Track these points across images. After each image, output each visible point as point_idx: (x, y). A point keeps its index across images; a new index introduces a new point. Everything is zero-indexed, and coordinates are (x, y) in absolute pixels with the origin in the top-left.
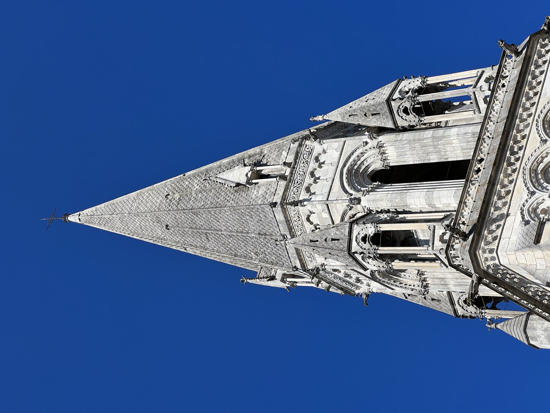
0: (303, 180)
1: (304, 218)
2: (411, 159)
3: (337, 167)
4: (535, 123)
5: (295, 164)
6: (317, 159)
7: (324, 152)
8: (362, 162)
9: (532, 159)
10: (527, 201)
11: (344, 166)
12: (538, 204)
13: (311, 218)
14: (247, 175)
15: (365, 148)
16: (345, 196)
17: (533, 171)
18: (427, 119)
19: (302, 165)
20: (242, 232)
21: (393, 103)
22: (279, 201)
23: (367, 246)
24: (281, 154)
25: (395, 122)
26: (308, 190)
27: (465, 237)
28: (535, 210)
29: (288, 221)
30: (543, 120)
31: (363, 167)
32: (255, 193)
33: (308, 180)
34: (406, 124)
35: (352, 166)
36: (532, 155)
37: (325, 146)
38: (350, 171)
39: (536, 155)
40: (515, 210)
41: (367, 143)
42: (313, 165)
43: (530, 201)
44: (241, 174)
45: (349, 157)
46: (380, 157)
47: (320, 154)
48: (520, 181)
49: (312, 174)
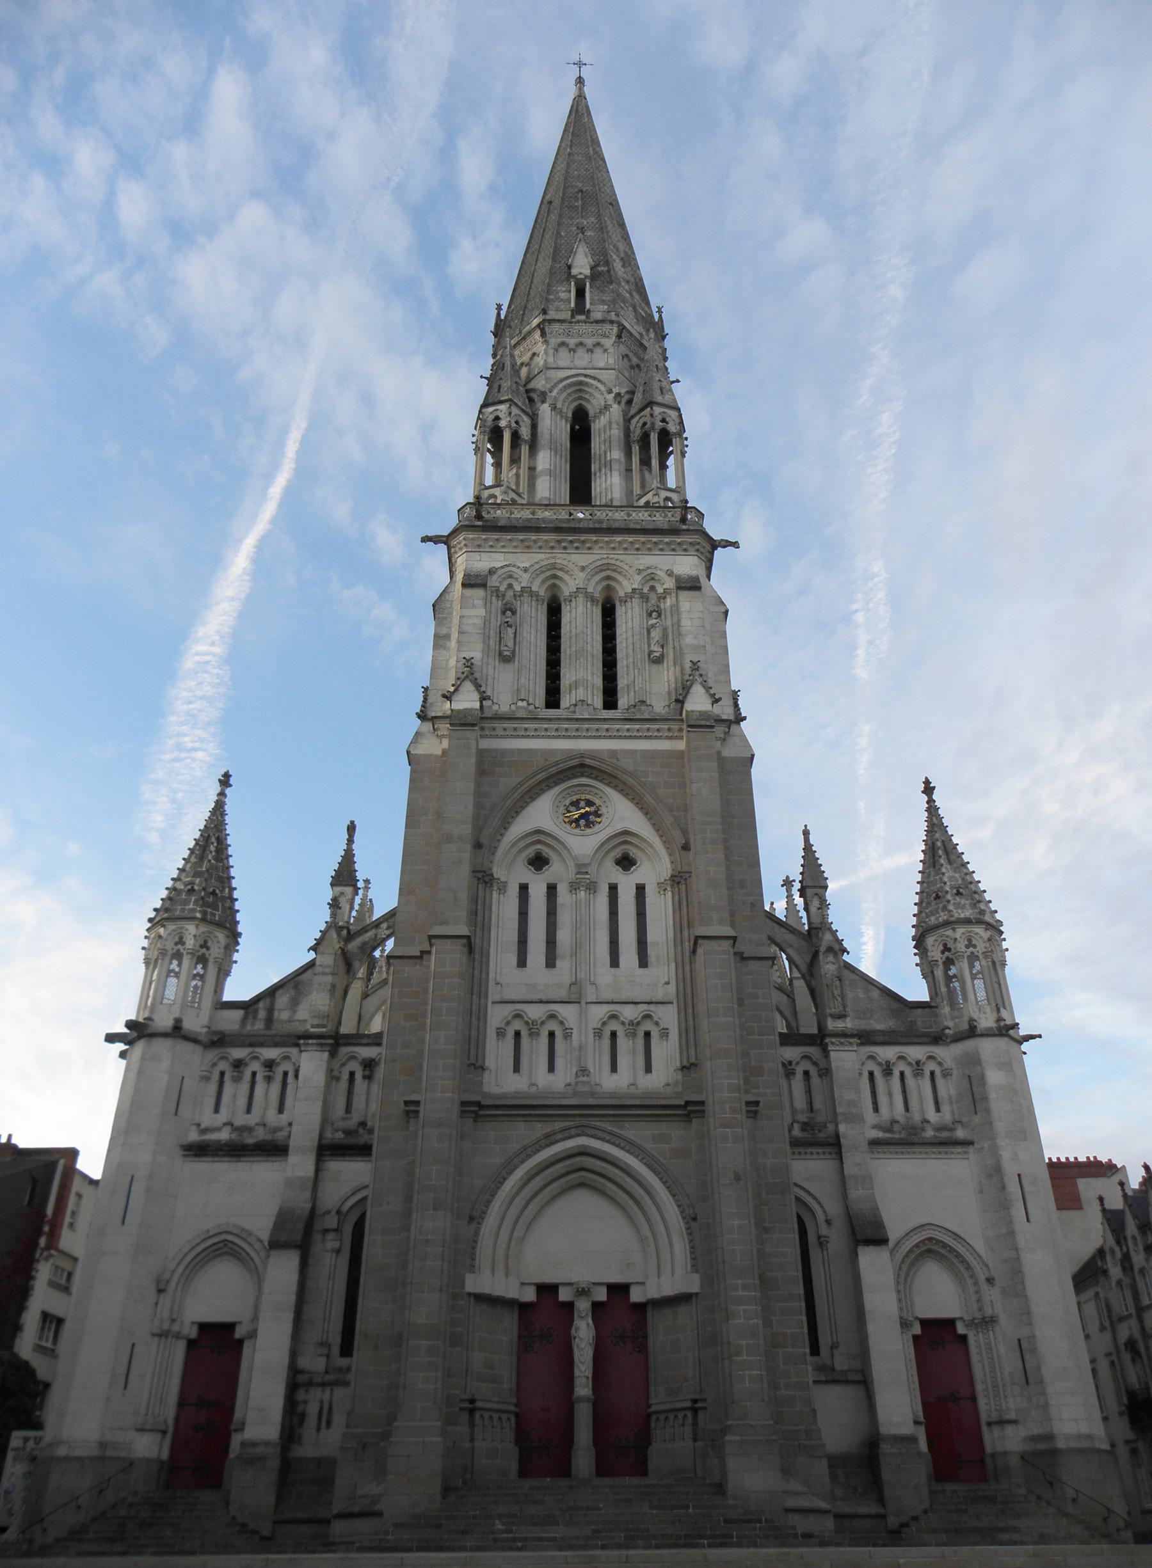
0: (573, 337)
1: (534, 350)
2: (597, 445)
3: (585, 369)
4: (605, 556)
5: (590, 323)
6: (598, 344)
7: (605, 350)
8: (591, 395)
9: (565, 563)
10: (519, 567)
11: (586, 376)
12: (517, 579)
13: (536, 358)
14: (581, 273)
15: (605, 393)
16: (548, 386)
17: (553, 567)
18: (636, 449)
19: (590, 330)
20: (530, 288)
21: (649, 409)
22: (548, 317)
23: (489, 423)
24: (607, 304)
25: (633, 417)
26: (563, 344)
27: (479, 517)
28: (511, 577)
29: (530, 333)
30: (608, 564)
31: (587, 396)
32: (564, 289)
33: (572, 342)
34: (632, 428)
35: (587, 384)
36: (569, 561)
37: (611, 350)
38: (581, 383)
39: (571, 566)
40: (512, 559)
41: (610, 392)
42: (589, 342)
43: (518, 571)
44: (582, 267)
45: (594, 378)
46: (598, 411)
47: (602, 346)
48: (543, 556)
49: (581, 344)
